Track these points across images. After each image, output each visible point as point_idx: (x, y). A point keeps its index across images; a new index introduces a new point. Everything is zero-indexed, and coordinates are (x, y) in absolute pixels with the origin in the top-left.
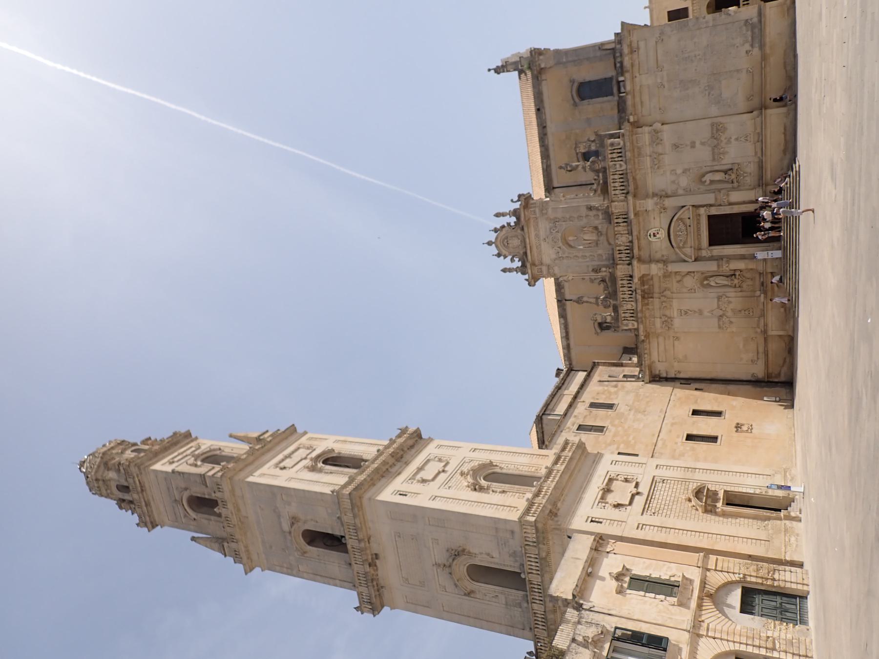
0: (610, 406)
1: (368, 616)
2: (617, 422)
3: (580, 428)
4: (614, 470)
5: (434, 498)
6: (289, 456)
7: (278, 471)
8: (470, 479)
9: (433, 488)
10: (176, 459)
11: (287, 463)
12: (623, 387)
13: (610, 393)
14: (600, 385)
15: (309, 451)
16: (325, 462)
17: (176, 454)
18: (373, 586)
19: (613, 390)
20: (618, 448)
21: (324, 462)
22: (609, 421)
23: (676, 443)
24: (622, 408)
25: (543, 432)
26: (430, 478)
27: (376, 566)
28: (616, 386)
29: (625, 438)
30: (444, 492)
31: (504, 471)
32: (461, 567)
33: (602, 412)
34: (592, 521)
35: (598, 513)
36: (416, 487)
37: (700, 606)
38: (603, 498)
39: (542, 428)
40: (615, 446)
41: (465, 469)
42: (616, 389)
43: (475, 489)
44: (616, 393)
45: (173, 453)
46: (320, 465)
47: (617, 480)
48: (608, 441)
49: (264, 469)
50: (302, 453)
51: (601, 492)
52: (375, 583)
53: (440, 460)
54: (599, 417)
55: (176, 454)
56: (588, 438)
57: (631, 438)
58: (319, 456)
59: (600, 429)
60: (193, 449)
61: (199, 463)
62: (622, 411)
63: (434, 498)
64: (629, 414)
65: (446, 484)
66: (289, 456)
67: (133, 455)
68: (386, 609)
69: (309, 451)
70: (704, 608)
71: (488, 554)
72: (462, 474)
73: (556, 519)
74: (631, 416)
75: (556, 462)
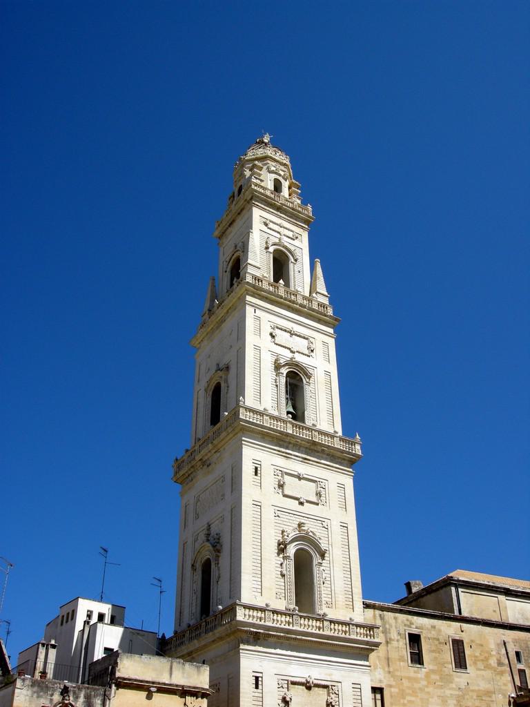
0: (461, 662)
1: (171, 472)
2: (434, 677)
3: (415, 640)
4: (346, 691)
5: (258, 505)
6: (292, 333)
7: (266, 329)
8: (292, 535)
9: (272, 498)
10: (271, 225)
11: (282, 337)
12: (502, 673)
13: (487, 659)
14: (498, 645)
15: (306, 352)
16: (291, 375)
18: (189, 470)
19: (493, 662)
20: (390, 686)
21: (289, 375)
22: (431, 667)
24: (461, 678)
25: (437, 590)
26: (286, 493)
27: (203, 466)
28: (500, 664)
29: (408, 691)
30: (268, 514)
31: (315, 569)
32: (207, 553)
33: (448, 655)
34: (257, 678)
35: (269, 684)
36: (269, 479)
38: (294, 683)
39: (441, 588)
40: (394, 683)
41: (310, 526)
42: (496, 665)
43: (279, 544)
44: (488, 667)
45: (280, 217)
46: (284, 371)
47: (329, 695)
48: (398, 673)
49: (265, 316)
50: (301, 345)
51: (304, 680)
52: (192, 470)
53: (319, 494)
54: (437, 656)
56: (402, 648)
57: (408, 698)
58: (297, 365)
59: (417, 658)
60: (291, 234)
61: (271, 249)
62: (457, 680)
63: (258, 505)
64: (452, 689)
65: (280, 512)
66: (292, 333)
67: (271, 186)
68: (178, 486)
69: (306, 352)
71: (219, 577)
72: (300, 525)
73: (251, 640)
74: (448, 692)
75: (331, 622)
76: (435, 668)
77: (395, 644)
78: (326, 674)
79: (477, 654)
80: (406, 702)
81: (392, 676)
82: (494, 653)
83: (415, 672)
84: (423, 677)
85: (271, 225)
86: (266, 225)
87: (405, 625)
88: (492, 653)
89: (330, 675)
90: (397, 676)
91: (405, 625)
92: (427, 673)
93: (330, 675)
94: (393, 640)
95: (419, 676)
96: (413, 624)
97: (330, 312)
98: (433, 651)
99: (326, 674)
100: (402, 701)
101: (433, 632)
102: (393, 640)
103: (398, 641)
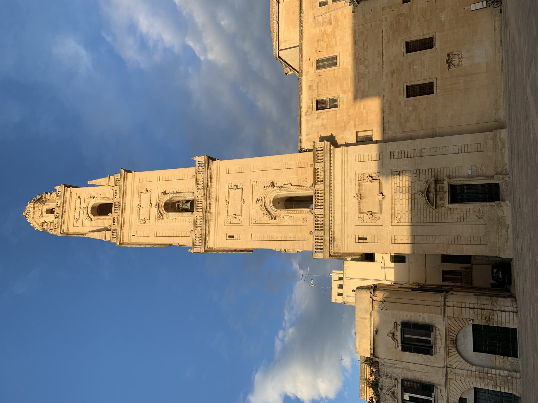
17: (72, 212)
20: (355, 126)
23: (400, 104)
37: (447, 354)
44: (333, 32)
45: (69, 211)
48: (345, 118)
51: (357, 202)
55: (72, 212)
62: (345, 65)
70: (450, 354)
76: (338, 85)
77: (325, 122)
78: (351, 184)
79: (325, 45)
80: (365, 111)
81: (348, 124)
82: (322, 29)
83: (343, 104)
84: (345, 96)
85: (77, 217)
86: (78, 219)
87: (311, 113)
88: (323, 31)
89: (351, 181)
90: (347, 119)
91: (311, 113)
92: (342, 93)
93: (351, 181)
94: (323, 123)
95: (345, 99)
96: (310, 106)
97: (118, 175)
98: (327, 87)
99: (351, 184)
100: (365, 115)
101: (314, 88)
102: (323, 123)
103: (323, 119)
